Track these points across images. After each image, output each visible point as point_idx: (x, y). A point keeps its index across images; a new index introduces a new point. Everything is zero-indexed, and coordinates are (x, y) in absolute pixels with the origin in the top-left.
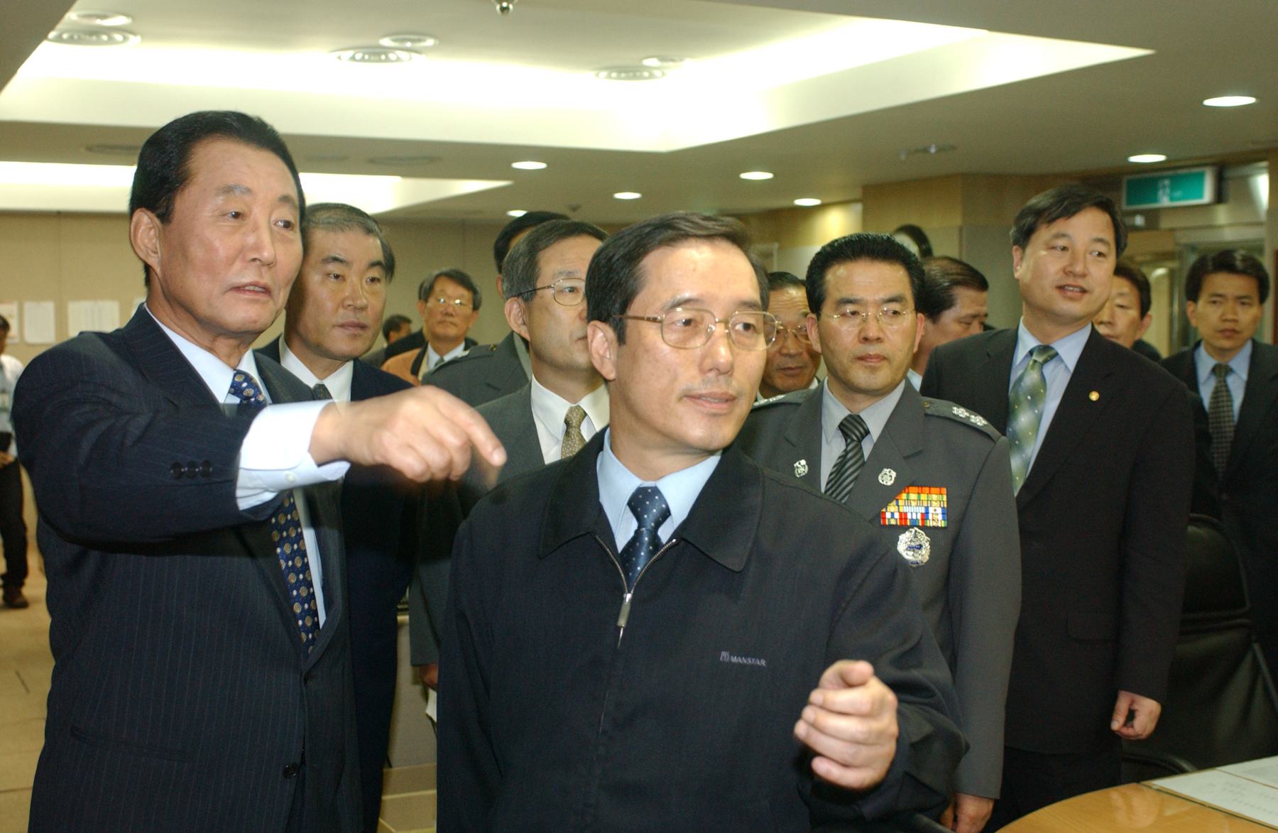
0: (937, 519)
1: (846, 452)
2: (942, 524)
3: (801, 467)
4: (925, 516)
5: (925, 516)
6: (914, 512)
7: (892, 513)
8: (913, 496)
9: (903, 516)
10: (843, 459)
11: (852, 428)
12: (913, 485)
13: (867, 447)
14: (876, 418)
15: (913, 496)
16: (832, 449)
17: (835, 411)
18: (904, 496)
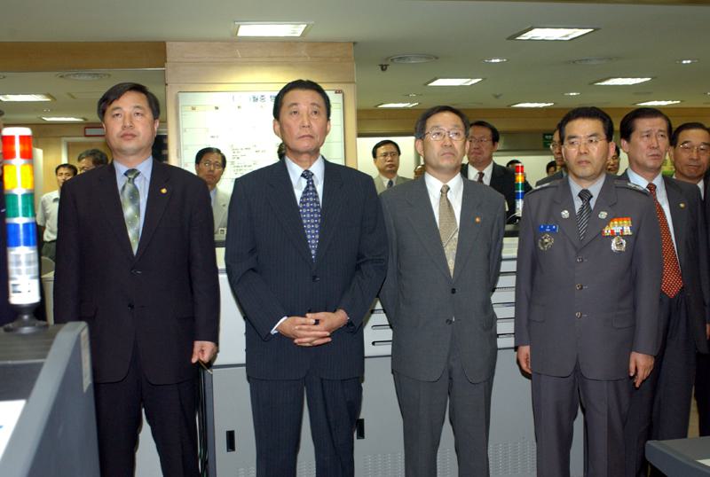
0: (628, 231)
1: (583, 206)
2: (630, 233)
3: (565, 214)
4: (622, 231)
5: (622, 231)
6: (617, 230)
7: (607, 231)
8: (616, 222)
9: (612, 231)
10: (582, 209)
11: (585, 195)
12: (614, 217)
13: (593, 203)
14: (595, 188)
15: (616, 222)
16: (578, 204)
17: (576, 188)
18: (612, 223)
